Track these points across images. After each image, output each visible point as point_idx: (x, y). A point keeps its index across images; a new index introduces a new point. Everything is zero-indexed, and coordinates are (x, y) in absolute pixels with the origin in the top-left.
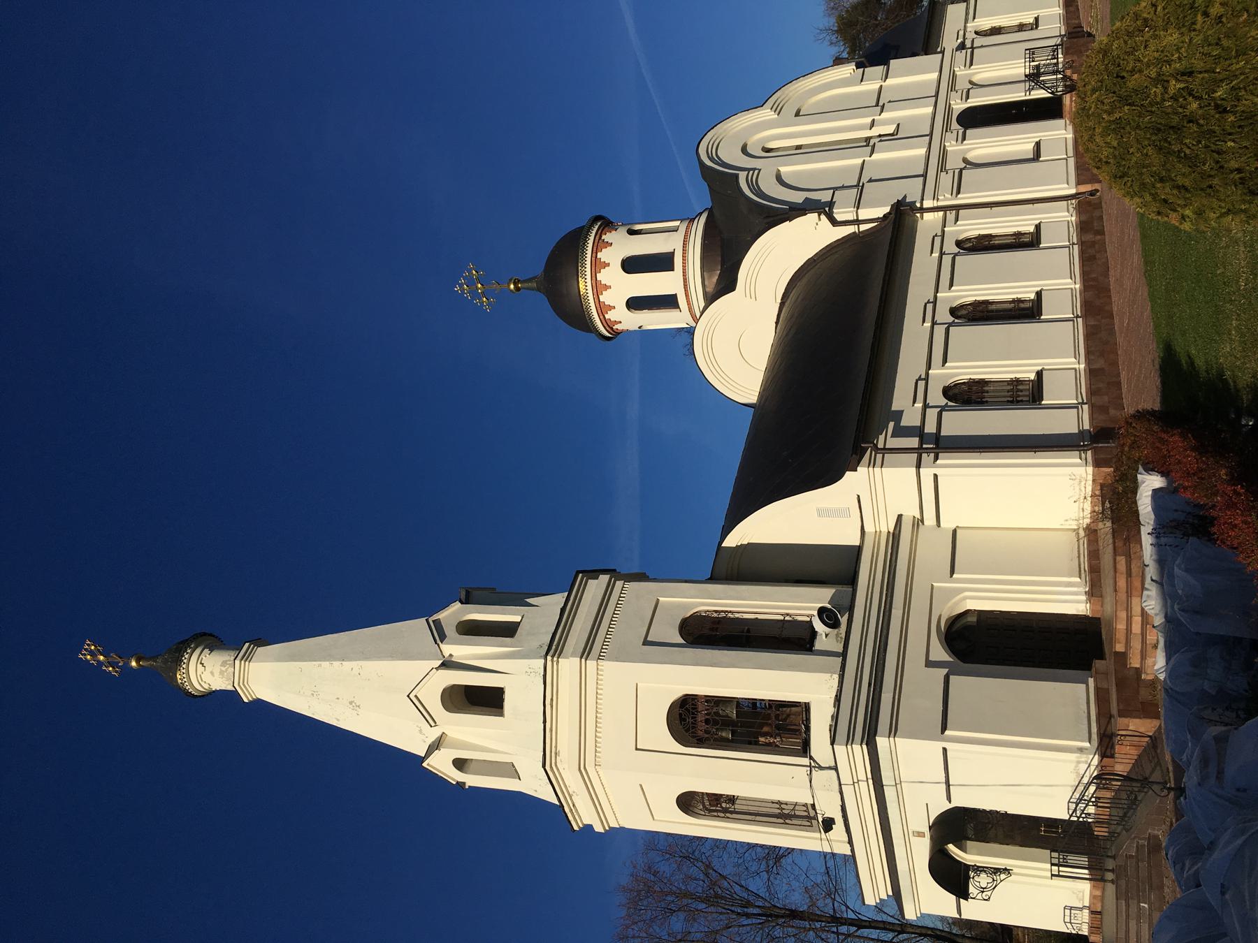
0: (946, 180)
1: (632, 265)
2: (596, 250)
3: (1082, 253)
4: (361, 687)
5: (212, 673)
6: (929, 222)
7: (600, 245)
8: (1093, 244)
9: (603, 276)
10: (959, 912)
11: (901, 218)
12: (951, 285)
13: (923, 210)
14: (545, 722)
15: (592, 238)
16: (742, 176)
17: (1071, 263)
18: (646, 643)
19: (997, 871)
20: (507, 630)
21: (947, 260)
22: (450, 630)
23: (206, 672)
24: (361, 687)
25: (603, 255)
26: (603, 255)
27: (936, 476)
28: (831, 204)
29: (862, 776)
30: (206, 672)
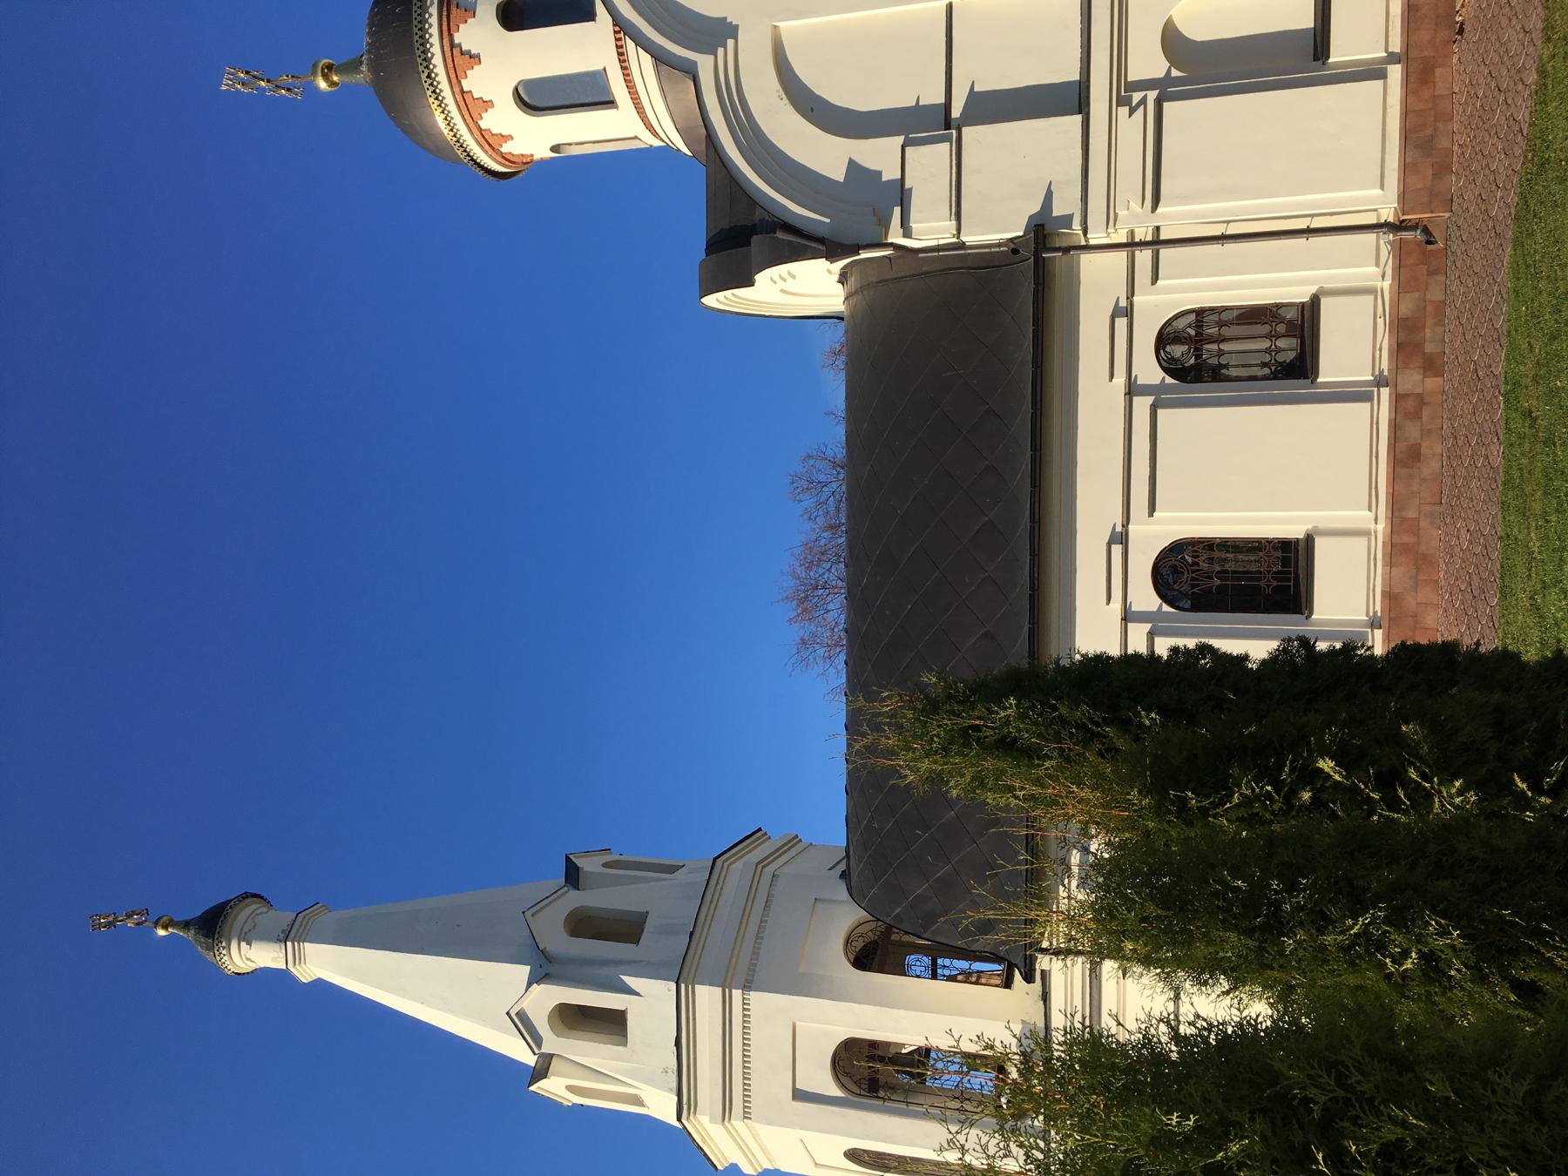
0: (1132, 128)
1: (537, 98)
2: (455, 77)
3: (1395, 427)
6: (1098, 279)
7: (461, 60)
8: (1421, 400)
9: (489, 121)
11: (1043, 250)
12: (1152, 509)
13: (1088, 248)
15: (436, 49)
16: (704, 63)
17: (1374, 455)
18: (799, 1095)
20: (612, 1024)
21: (1142, 404)
22: (543, 1027)
25: (474, 82)
26: (474, 82)
28: (901, 194)
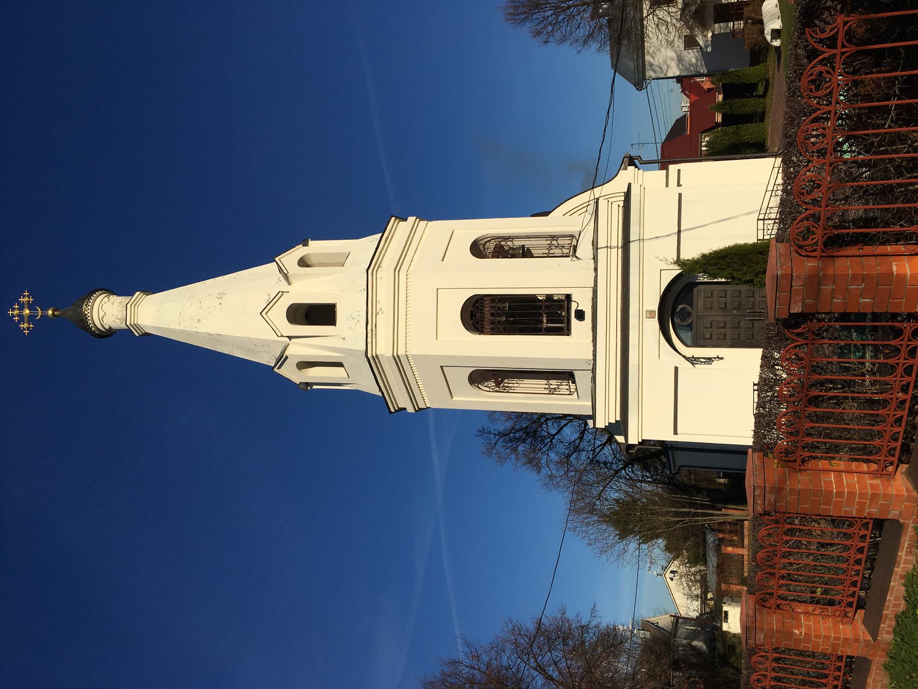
4: (224, 312)
5: (113, 303)
10: (676, 433)
14: (377, 249)
19: (709, 360)
23: (106, 311)
24: (224, 312)
27: (679, 170)
29: (614, 244)
30: (106, 311)
